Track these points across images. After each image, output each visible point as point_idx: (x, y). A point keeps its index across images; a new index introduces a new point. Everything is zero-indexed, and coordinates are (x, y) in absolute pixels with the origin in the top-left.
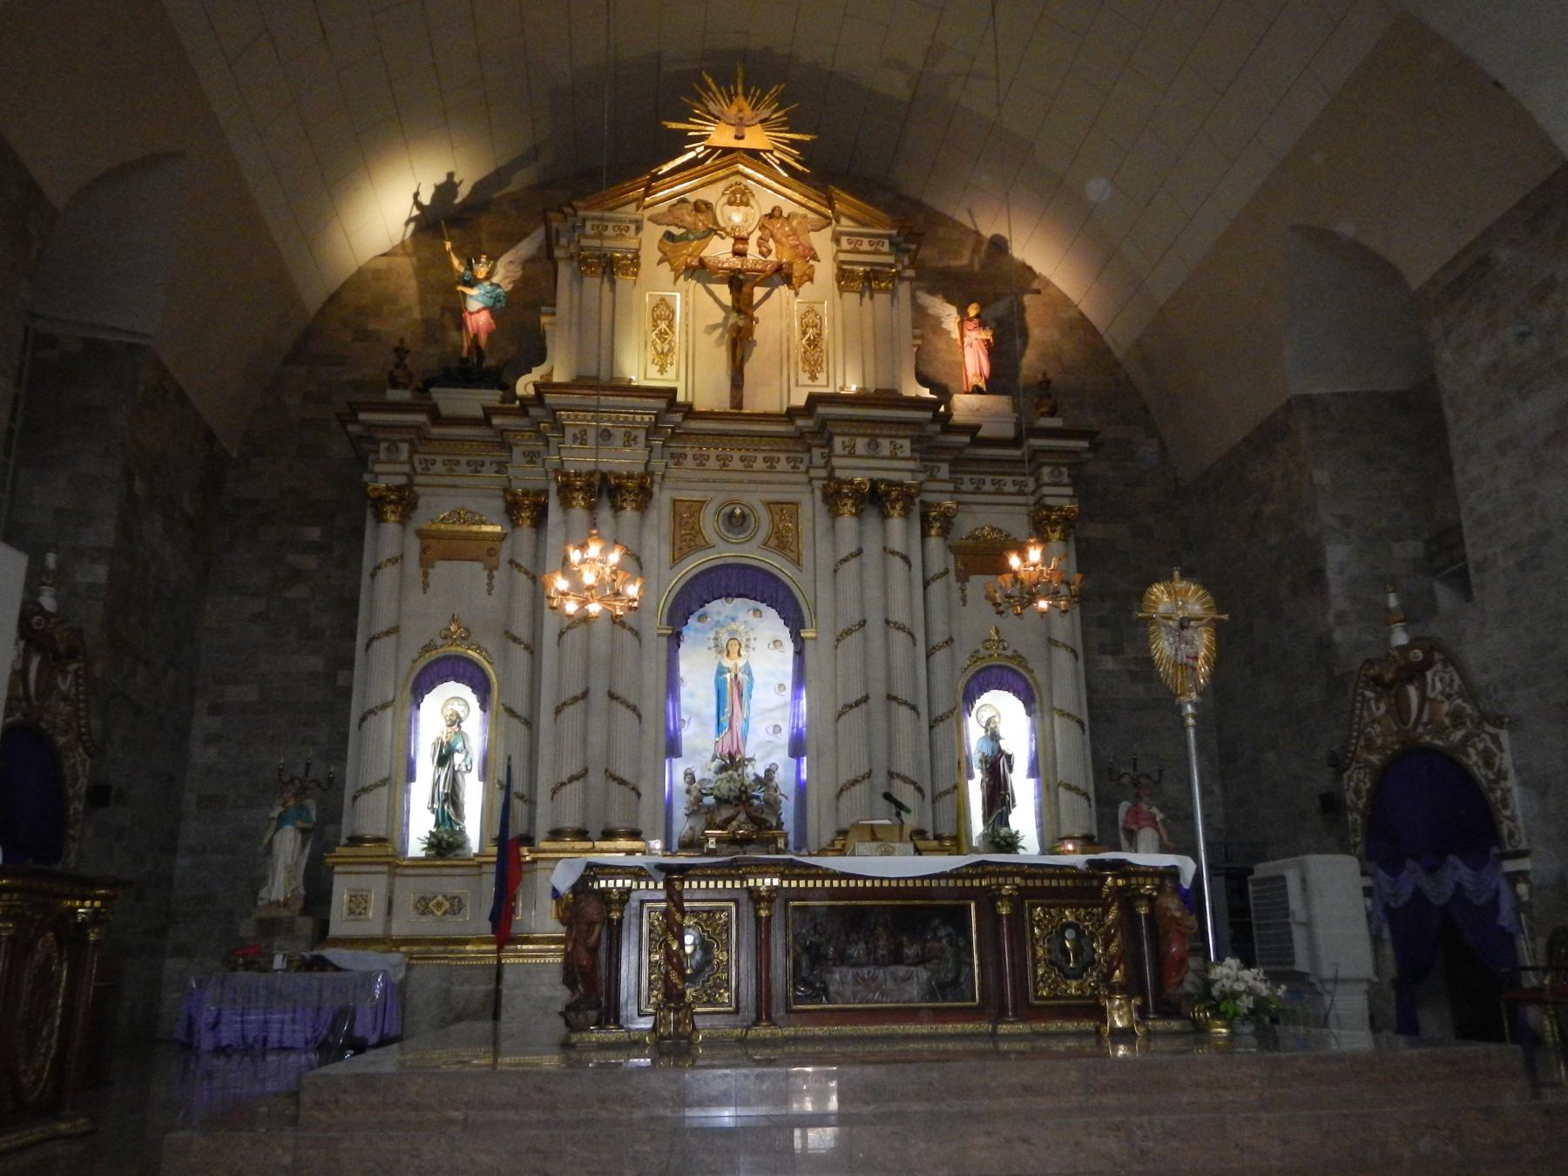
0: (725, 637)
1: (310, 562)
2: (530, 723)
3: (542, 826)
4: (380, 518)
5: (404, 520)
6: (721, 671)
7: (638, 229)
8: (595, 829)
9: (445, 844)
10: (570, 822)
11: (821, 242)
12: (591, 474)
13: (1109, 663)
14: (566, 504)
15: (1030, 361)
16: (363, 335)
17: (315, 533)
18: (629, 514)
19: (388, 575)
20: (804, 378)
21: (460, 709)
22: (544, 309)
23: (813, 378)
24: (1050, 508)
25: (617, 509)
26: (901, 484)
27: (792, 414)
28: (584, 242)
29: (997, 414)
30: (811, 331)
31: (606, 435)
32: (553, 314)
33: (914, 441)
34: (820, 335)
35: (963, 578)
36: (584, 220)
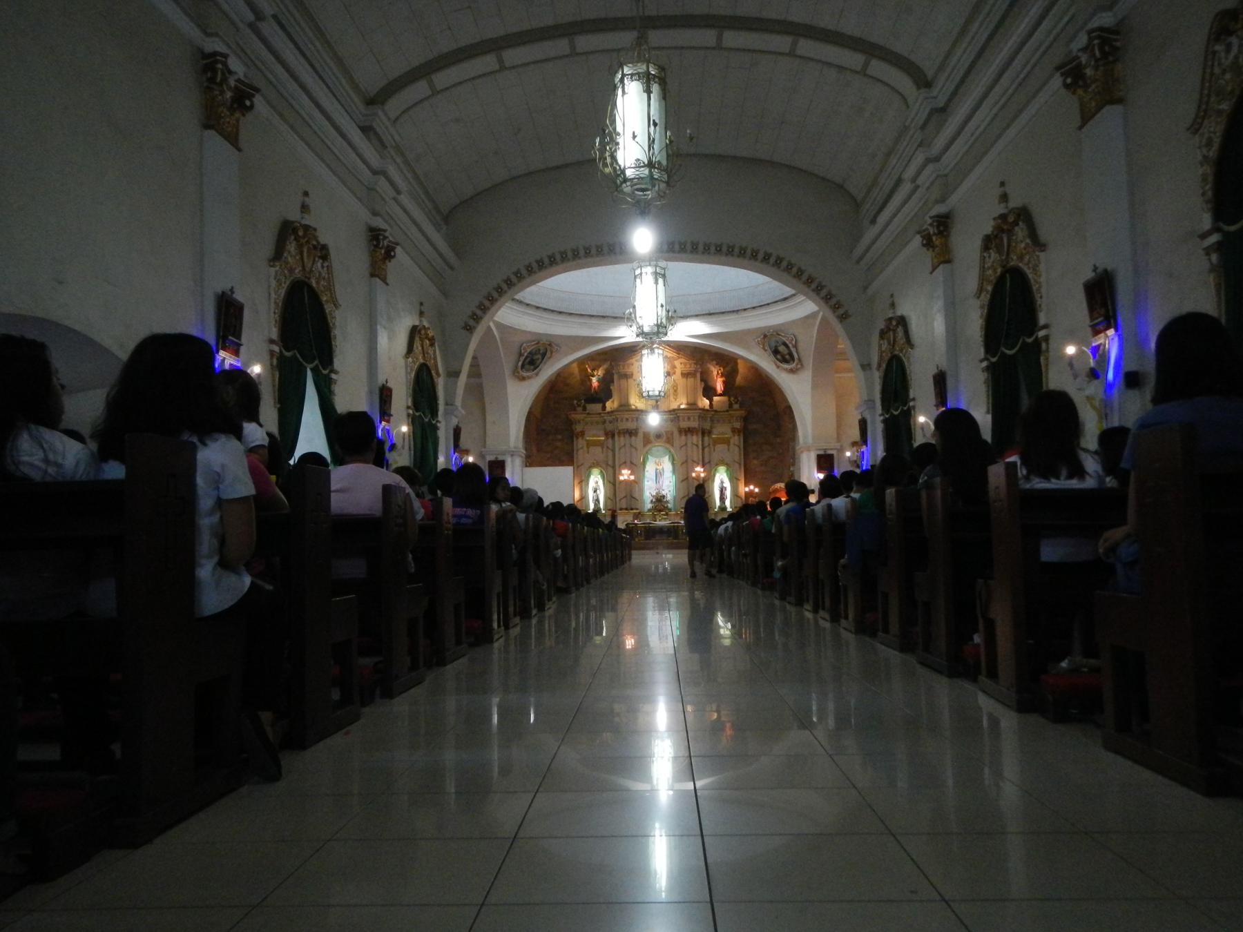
0: (657, 461)
1: (559, 444)
2: (614, 485)
3: (618, 506)
4: (577, 438)
5: (583, 439)
6: (656, 469)
7: (632, 365)
8: (629, 508)
9: (597, 511)
10: (624, 506)
11: (677, 363)
12: (624, 429)
13: (755, 462)
14: (619, 437)
15: (739, 380)
16: (567, 385)
17: (560, 437)
18: (633, 438)
19: (581, 452)
20: (673, 400)
21: (596, 479)
22: (612, 384)
23: (676, 400)
24: (734, 428)
25: (631, 436)
26: (695, 428)
27: (670, 411)
28: (620, 371)
29: (724, 402)
30: (675, 388)
31: (627, 419)
32: (613, 385)
33: (699, 417)
34: (677, 388)
35: (714, 445)
36: (619, 365)
